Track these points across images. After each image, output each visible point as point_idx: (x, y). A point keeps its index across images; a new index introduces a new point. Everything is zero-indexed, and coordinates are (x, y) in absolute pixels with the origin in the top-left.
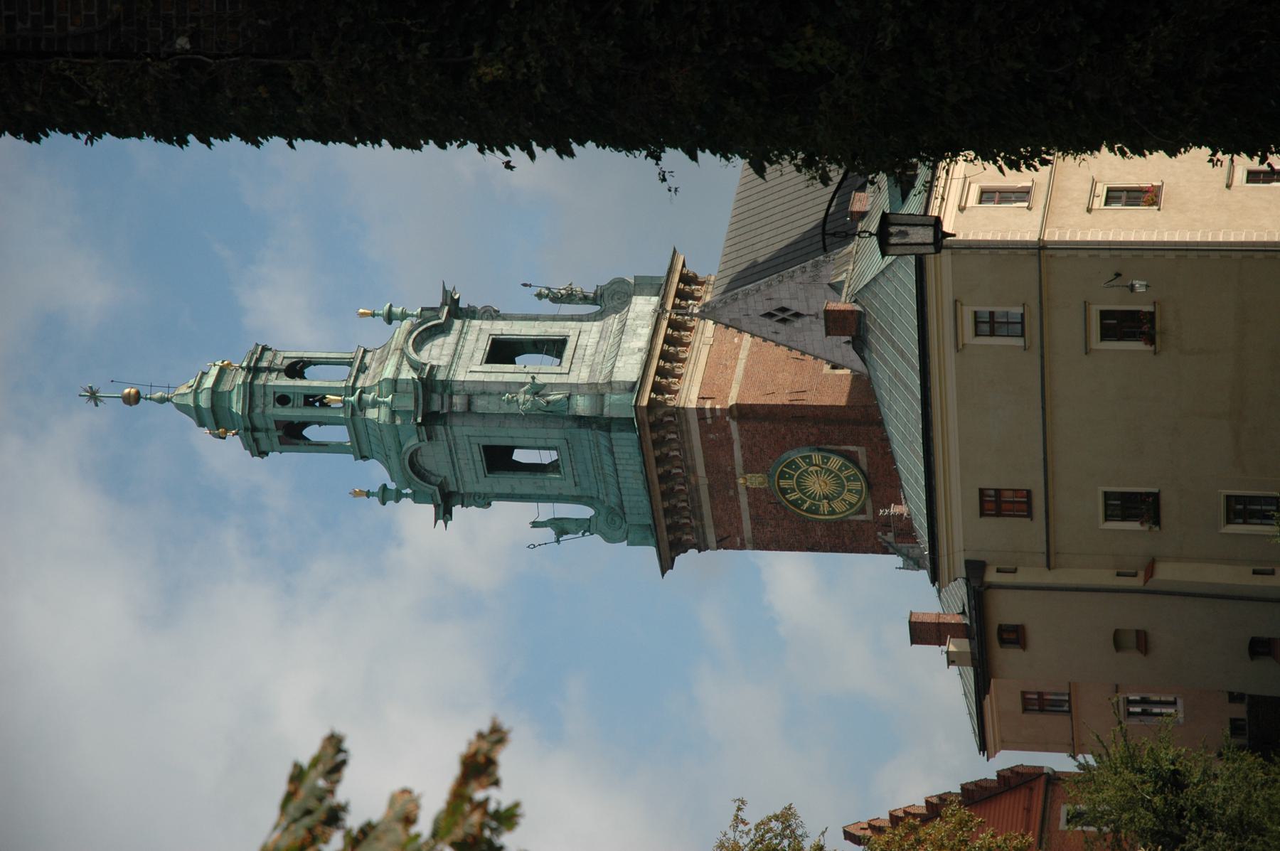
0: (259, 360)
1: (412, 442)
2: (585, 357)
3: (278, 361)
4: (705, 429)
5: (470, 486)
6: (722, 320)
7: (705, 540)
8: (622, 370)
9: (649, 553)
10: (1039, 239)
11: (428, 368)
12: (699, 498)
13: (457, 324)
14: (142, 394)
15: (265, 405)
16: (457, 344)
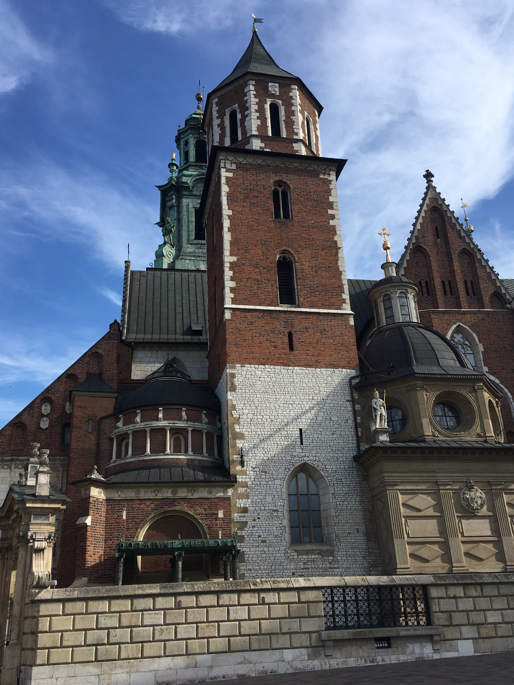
2: (201, 250)
8: (183, 263)
15: (183, 138)
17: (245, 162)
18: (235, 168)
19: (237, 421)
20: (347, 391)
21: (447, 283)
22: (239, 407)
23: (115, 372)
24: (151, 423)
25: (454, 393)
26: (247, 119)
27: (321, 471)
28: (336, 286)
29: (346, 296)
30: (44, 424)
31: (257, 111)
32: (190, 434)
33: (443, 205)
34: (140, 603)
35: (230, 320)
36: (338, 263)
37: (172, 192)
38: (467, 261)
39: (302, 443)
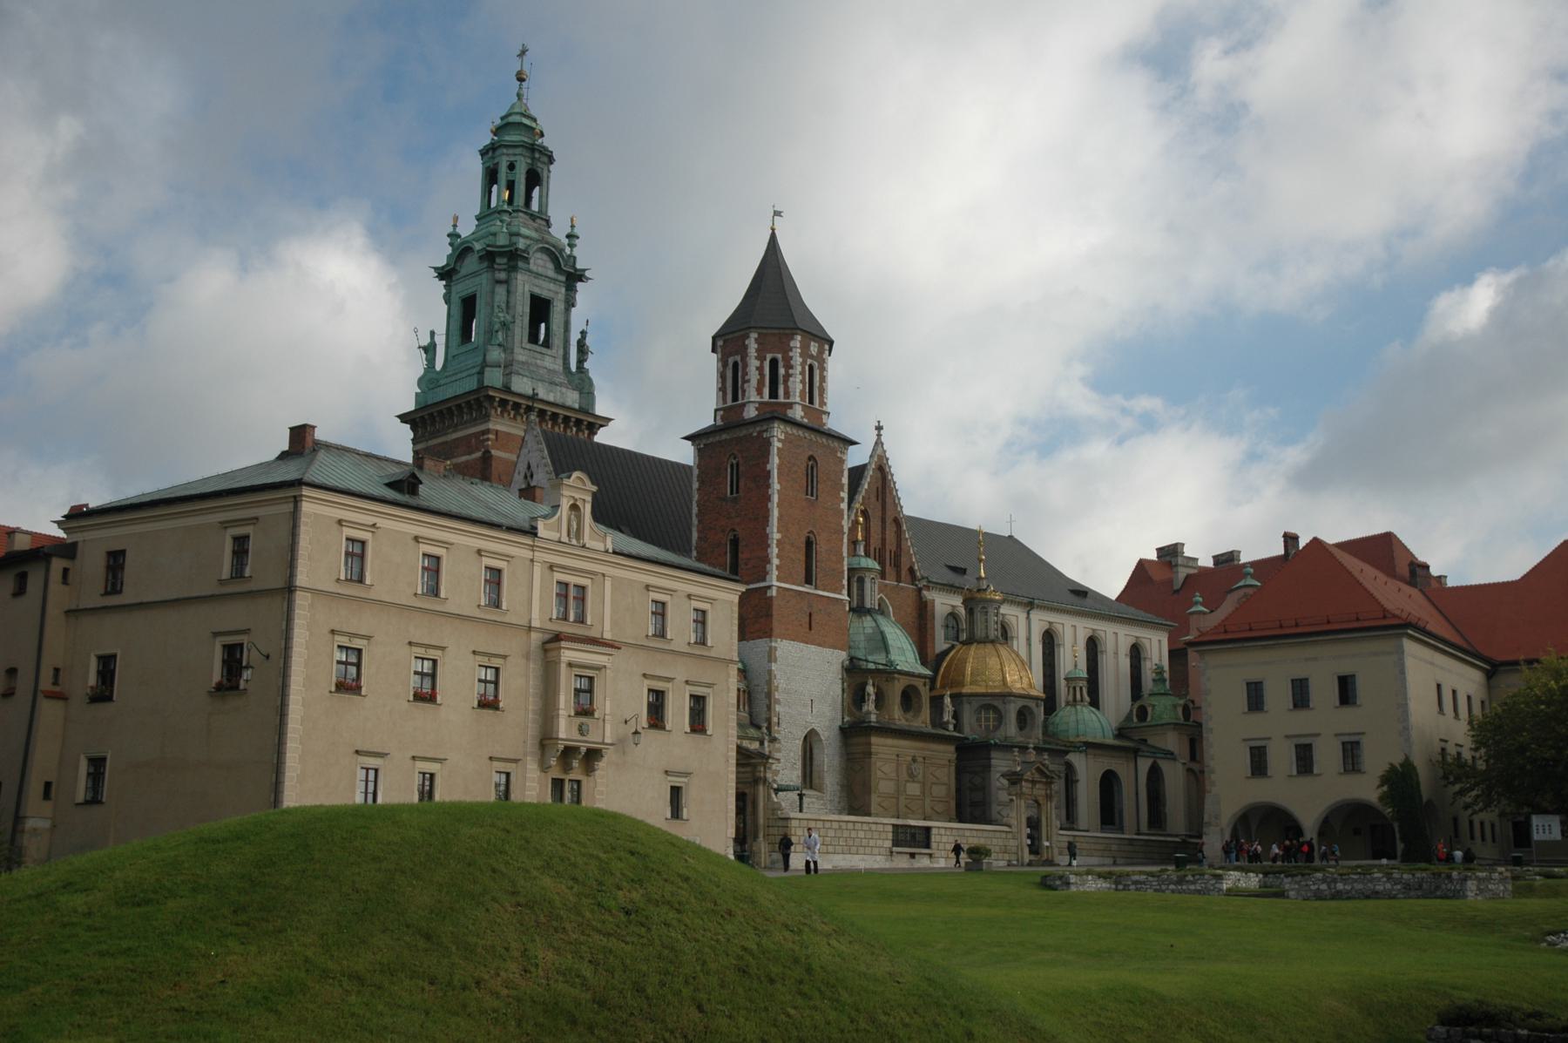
0: (541, 151)
1: (477, 246)
2: (533, 360)
3: (539, 164)
4: (477, 435)
5: (454, 289)
6: (527, 435)
7: (418, 443)
8: (520, 381)
9: (413, 408)
10: (296, 587)
11: (526, 255)
12: (440, 436)
13: (563, 278)
14: (523, 83)
15: (508, 155)
16: (546, 277)
20: (840, 672)
21: (877, 551)
22: (778, 677)
26: (791, 379)
29: (845, 582)
36: (841, 549)
37: (505, 260)
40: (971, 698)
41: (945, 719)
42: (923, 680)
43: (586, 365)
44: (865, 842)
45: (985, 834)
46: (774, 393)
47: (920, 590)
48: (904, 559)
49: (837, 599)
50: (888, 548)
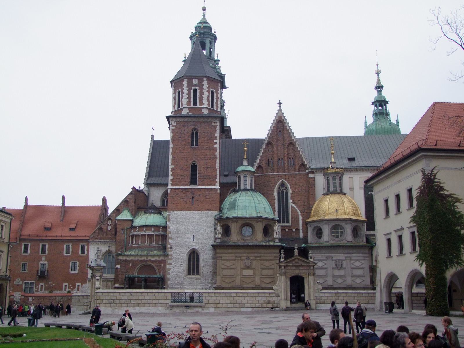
3: (204, 39)
15: (193, 40)
17: (180, 121)
18: (176, 124)
19: (170, 232)
20: (213, 220)
23: (134, 208)
24: (141, 232)
25: (249, 223)
26: (183, 98)
27: (200, 251)
28: (214, 176)
29: (218, 180)
30: (109, 228)
31: (187, 95)
32: (154, 236)
33: (284, 120)
34: (122, 294)
35: (170, 193)
38: (292, 148)
39: (193, 241)
40: (311, 224)
41: (275, 237)
42: (256, 220)
43: (224, 108)
44: (149, 301)
45: (249, 295)
46: (179, 107)
47: (308, 174)
48: (296, 161)
49: (211, 189)
50: (286, 157)
